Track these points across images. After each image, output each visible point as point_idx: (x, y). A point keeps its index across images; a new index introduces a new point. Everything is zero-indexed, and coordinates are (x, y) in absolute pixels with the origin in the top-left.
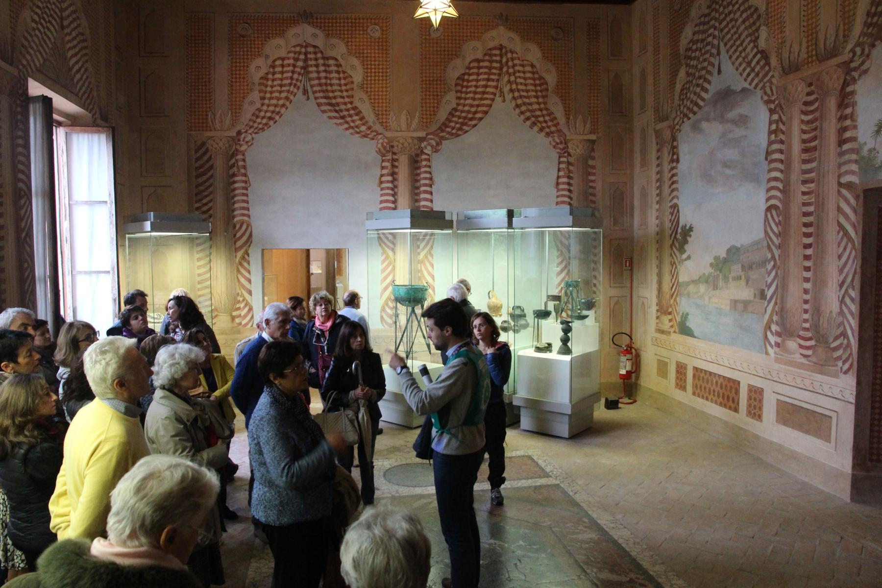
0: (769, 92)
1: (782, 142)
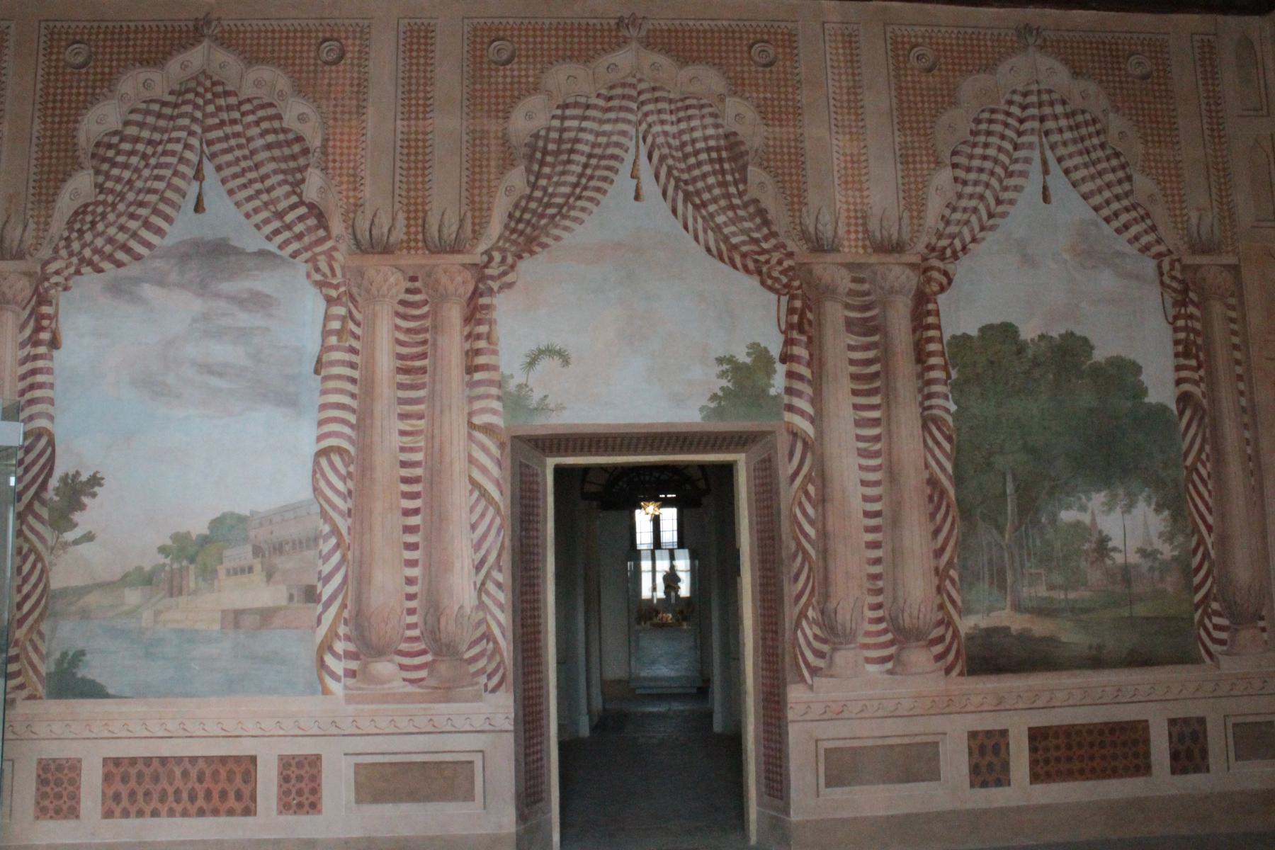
0: (326, 269)
1: (353, 350)
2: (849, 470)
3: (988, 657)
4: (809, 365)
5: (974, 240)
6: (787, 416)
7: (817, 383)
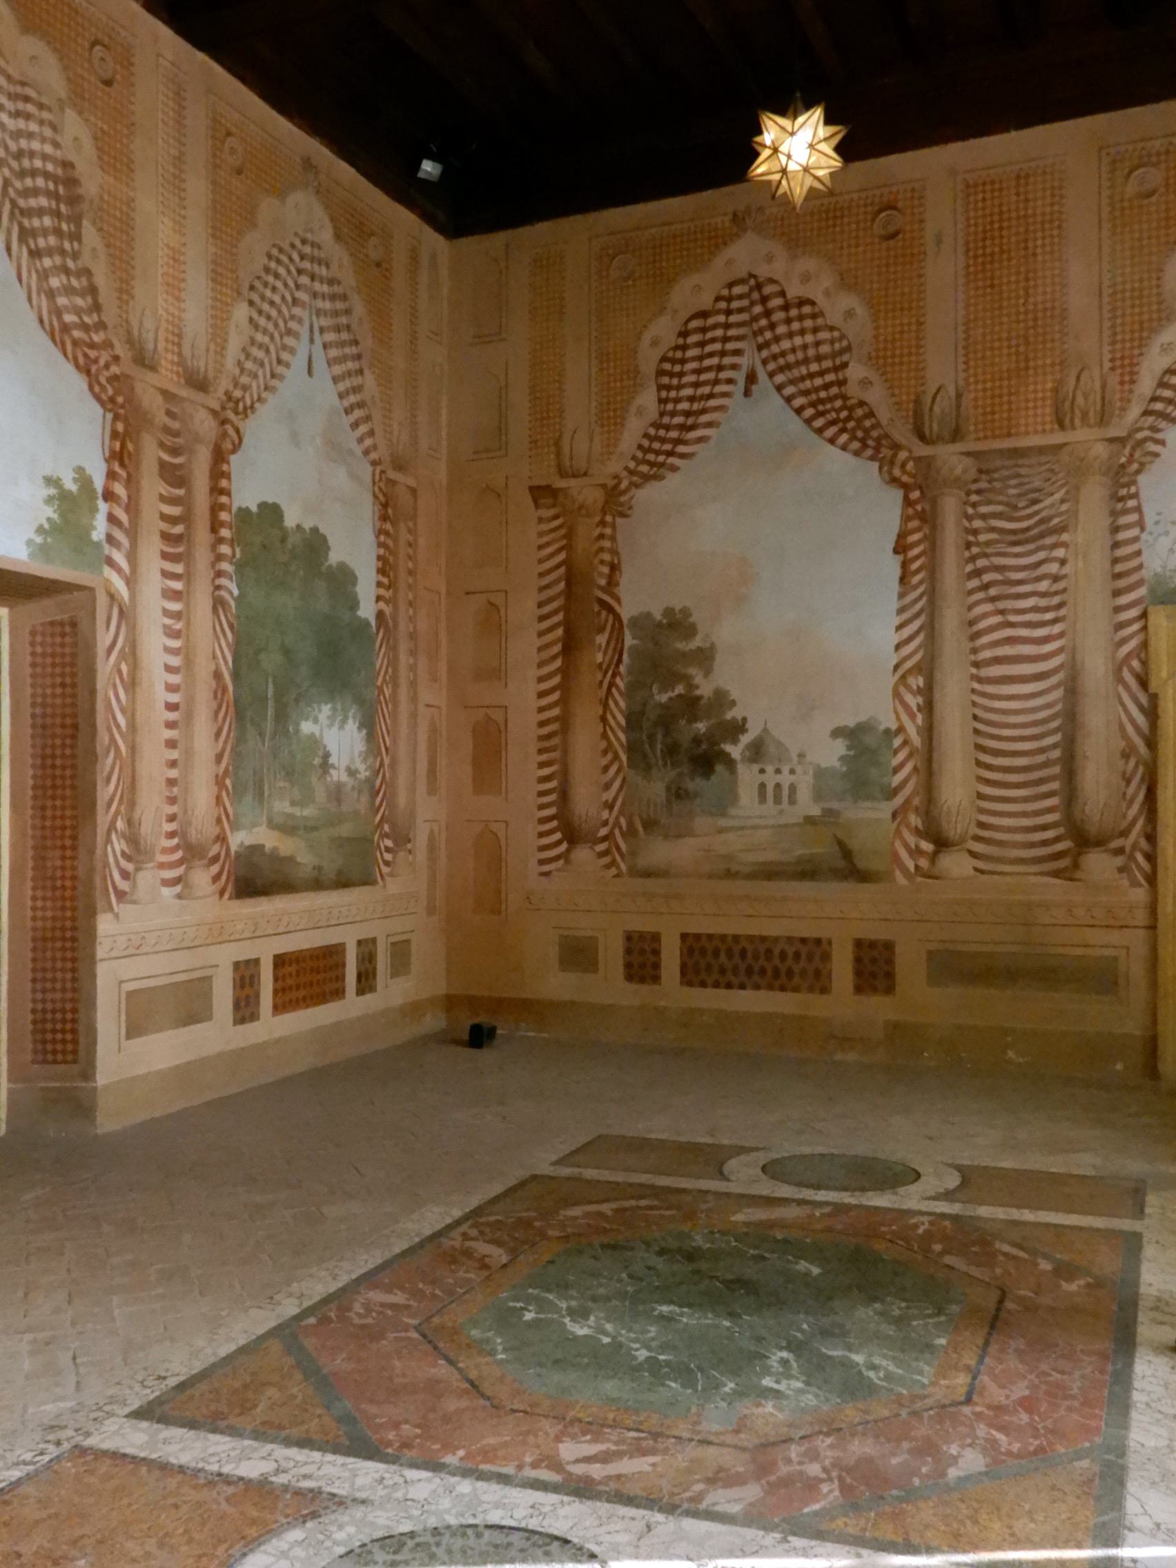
2: (155, 648)
3: (253, 879)
4: (127, 509)
5: (259, 399)
6: (108, 572)
7: (133, 533)
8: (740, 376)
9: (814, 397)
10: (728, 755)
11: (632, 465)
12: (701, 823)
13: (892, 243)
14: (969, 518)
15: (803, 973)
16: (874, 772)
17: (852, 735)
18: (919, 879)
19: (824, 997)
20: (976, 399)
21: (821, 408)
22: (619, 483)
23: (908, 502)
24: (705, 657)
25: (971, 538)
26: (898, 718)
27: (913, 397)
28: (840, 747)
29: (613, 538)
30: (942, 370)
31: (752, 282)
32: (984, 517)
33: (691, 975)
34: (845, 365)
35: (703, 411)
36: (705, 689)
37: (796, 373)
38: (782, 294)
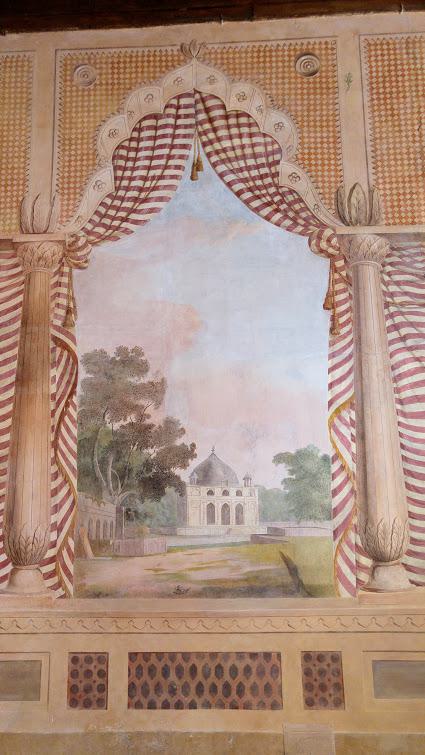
8: (188, 165)
9: (251, 184)
10: (178, 478)
11: (89, 227)
12: (150, 542)
13: (311, 79)
14: (387, 284)
15: (254, 688)
16: (315, 495)
17: (295, 461)
18: (360, 592)
19: (277, 712)
20: (385, 195)
21: (257, 192)
22: (78, 239)
23: (334, 269)
24: (156, 391)
25: (389, 299)
26: (335, 447)
27: (334, 190)
28: (283, 471)
29: (69, 286)
30: (355, 171)
31: (197, 96)
32: (398, 283)
33: (141, 696)
34: (278, 162)
35: (155, 188)
36: (156, 418)
37: (235, 165)
38: (223, 107)
